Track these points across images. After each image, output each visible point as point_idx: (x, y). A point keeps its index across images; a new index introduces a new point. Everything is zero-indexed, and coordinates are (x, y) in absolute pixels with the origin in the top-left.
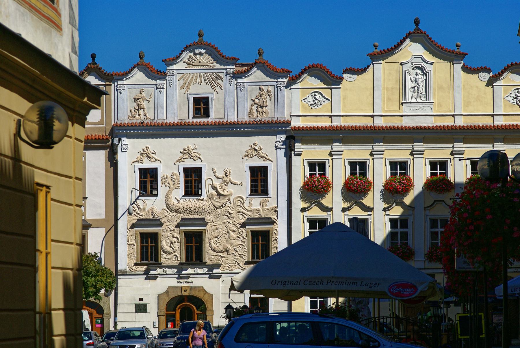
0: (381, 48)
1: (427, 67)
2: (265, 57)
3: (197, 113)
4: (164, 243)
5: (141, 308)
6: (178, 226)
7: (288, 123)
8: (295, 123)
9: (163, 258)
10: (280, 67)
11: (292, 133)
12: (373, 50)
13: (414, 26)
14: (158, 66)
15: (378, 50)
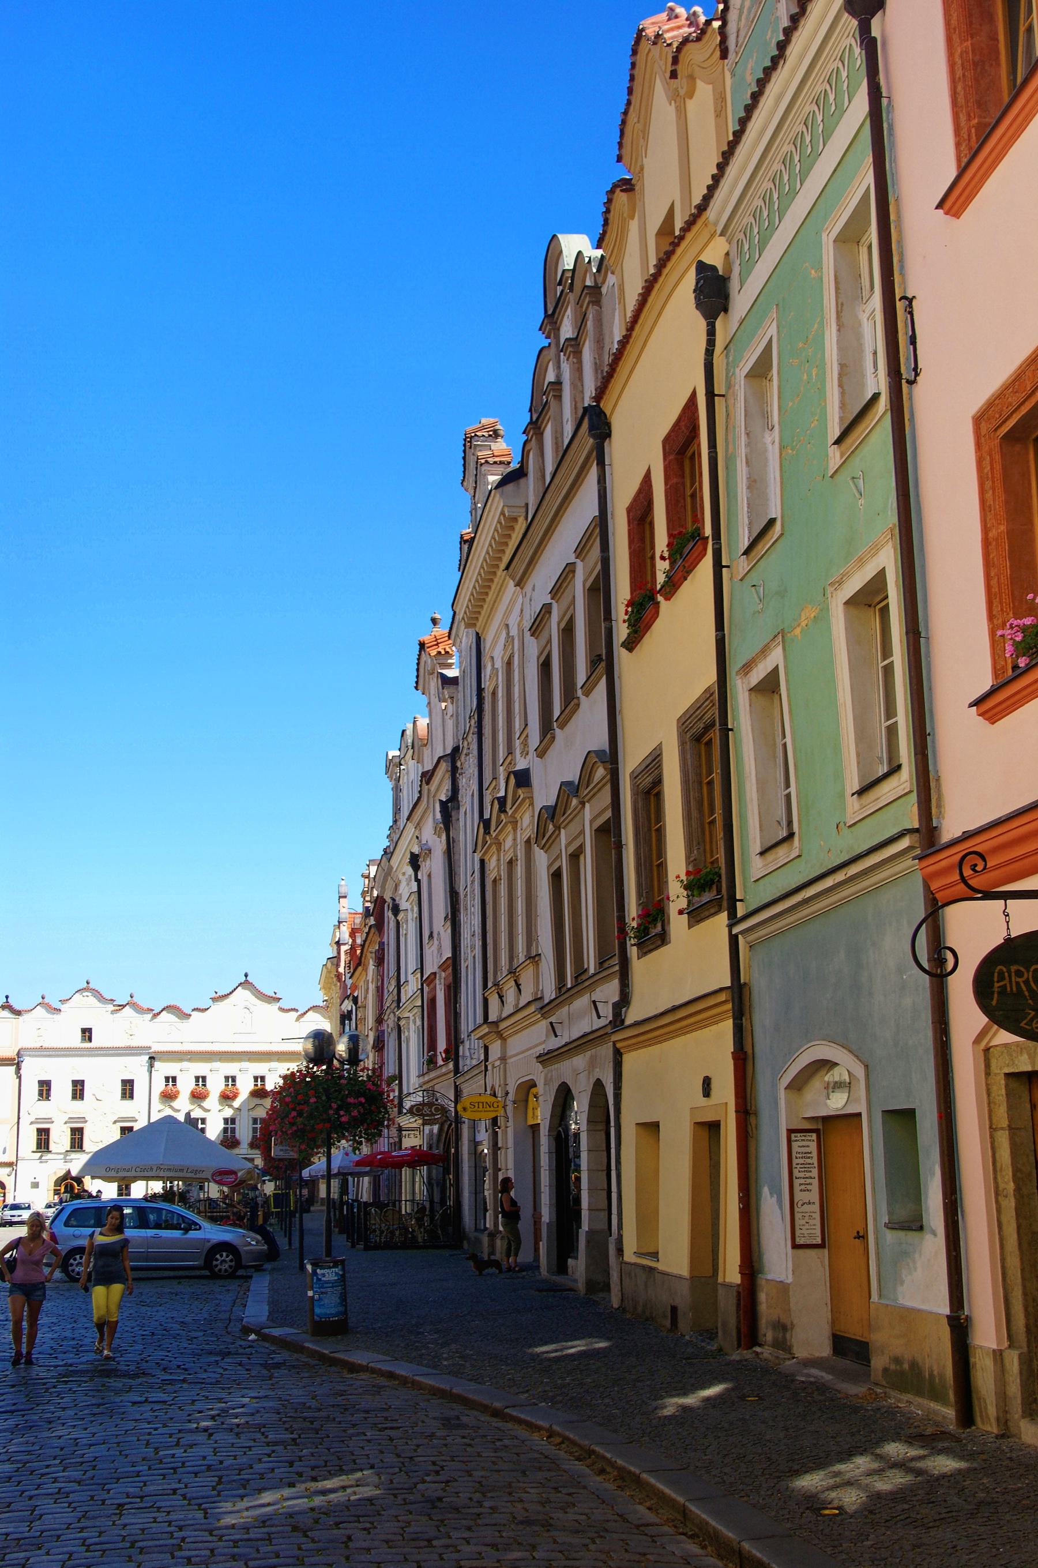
0: (220, 994)
1: (252, 1009)
2: (135, 999)
3: (83, 1039)
4: (53, 1137)
5: (35, 1185)
6: (66, 1123)
7: (150, 1048)
8: (156, 1048)
9: (52, 1147)
10: (146, 1006)
11: (153, 1055)
12: (214, 995)
13: (244, 978)
14: (56, 1005)
15: (217, 995)
